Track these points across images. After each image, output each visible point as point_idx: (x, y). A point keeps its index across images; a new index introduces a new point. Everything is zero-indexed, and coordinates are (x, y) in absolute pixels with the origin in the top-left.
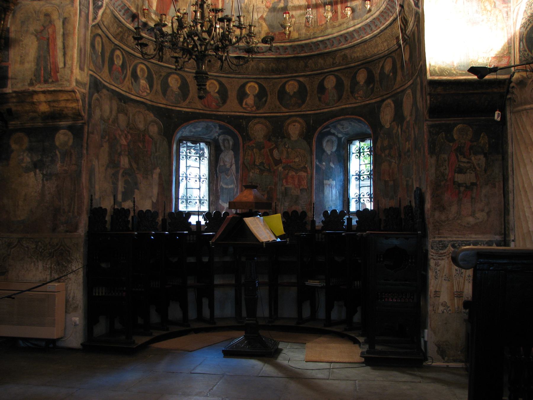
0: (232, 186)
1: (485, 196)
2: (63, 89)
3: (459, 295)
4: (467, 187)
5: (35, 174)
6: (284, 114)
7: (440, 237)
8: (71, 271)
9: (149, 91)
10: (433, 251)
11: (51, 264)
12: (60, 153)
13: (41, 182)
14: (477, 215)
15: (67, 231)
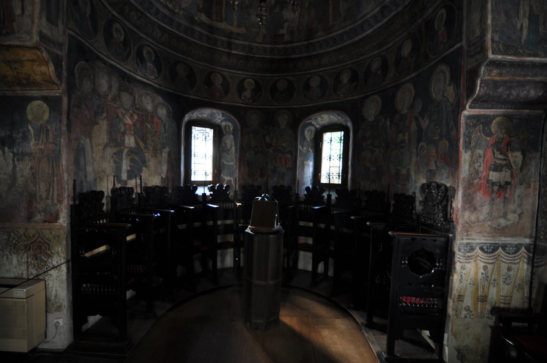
0: (232, 163)
1: (519, 196)
2: (22, 44)
3: (484, 299)
4: (501, 187)
5: (4, 152)
6: (275, 107)
7: (469, 239)
8: (51, 266)
9: (156, 75)
10: (460, 253)
11: (28, 258)
12: (33, 128)
13: (11, 162)
14: (509, 217)
15: (45, 221)
